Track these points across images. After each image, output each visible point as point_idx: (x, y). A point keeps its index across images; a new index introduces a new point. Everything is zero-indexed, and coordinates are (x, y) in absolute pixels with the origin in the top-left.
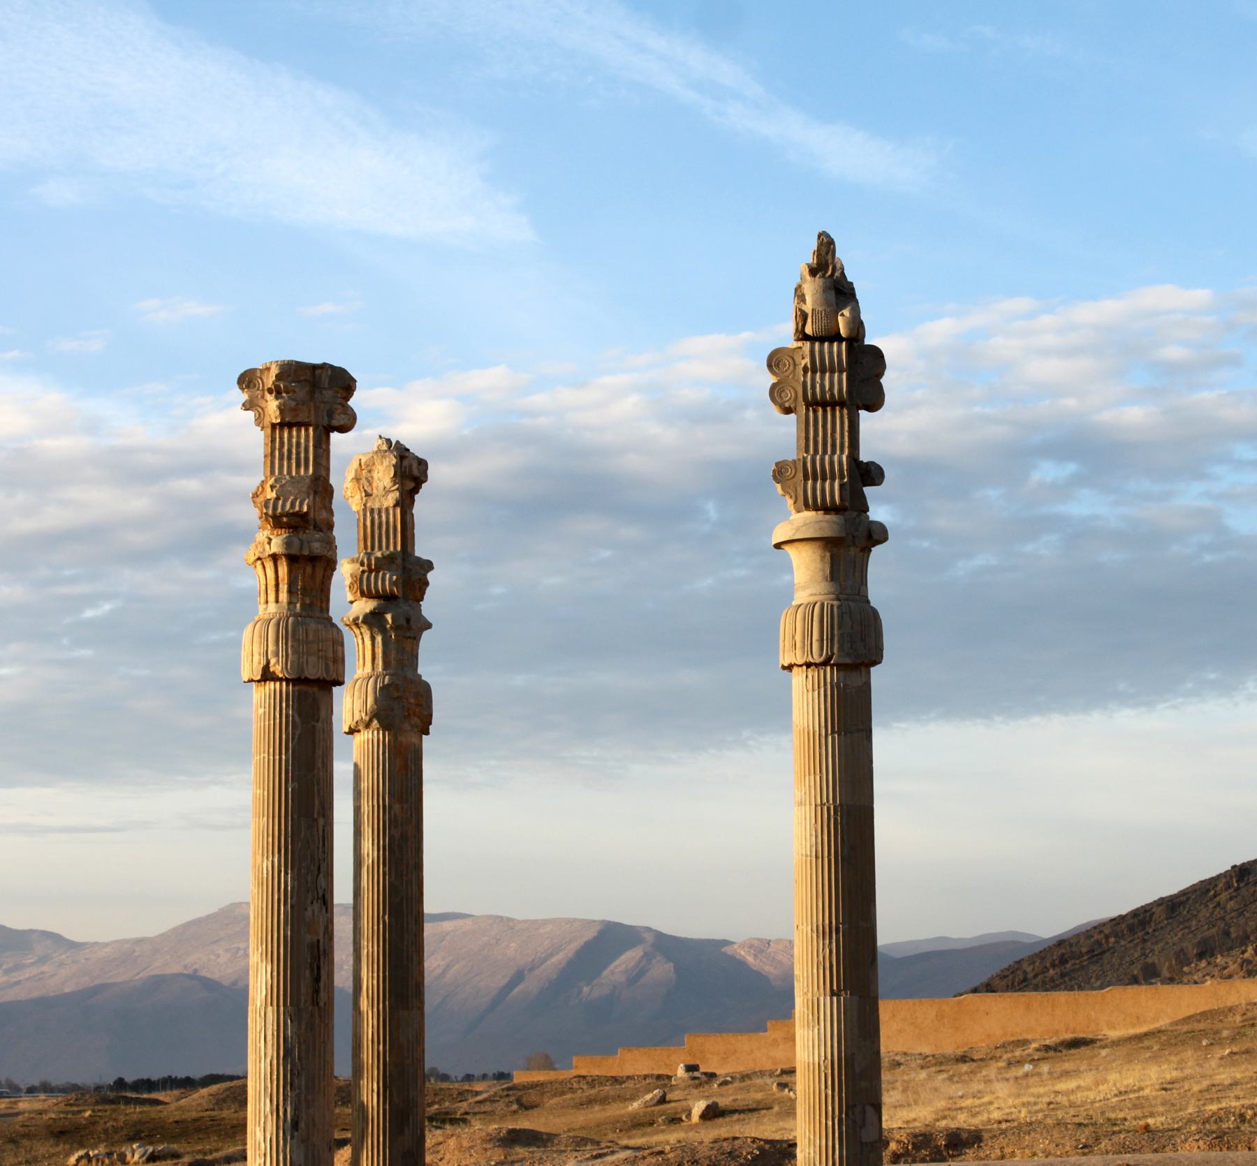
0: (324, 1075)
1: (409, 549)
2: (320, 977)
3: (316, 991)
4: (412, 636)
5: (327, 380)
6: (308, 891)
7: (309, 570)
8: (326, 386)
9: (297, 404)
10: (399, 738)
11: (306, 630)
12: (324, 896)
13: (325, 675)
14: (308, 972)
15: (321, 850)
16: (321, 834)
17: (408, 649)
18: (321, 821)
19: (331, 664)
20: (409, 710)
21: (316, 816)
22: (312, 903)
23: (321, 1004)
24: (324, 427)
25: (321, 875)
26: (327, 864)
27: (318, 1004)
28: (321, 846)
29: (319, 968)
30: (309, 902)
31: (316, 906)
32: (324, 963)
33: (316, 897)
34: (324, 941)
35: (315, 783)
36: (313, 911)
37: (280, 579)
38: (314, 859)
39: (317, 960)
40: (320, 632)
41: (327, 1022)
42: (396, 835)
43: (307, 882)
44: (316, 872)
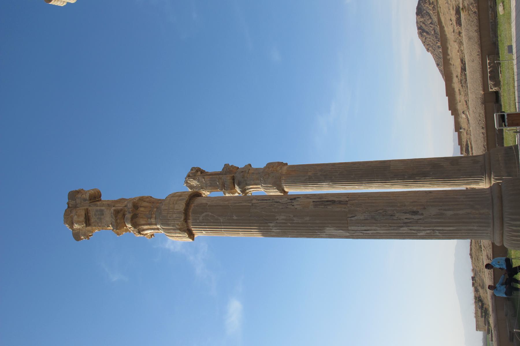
0: (387, 197)
2: (333, 200)
3: (340, 202)
4: (248, 170)
5: (73, 201)
6: (287, 208)
8: (75, 202)
9: (76, 215)
10: (284, 173)
11: (163, 210)
12: (291, 199)
14: (329, 207)
15: (268, 202)
16: (259, 201)
17: (252, 171)
18: (254, 201)
19: (181, 198)
20: (274, 170)
21: (250, 204)
22: (293, 205)
23: (347, 199)
25: (280, 201)
26: (276, 198)
27: (347, 201)
28: (266, 201)
29: (327, 201)
30: (292, 207)
31: (295, 203)
32: (326, 198)
33: (290, 203)
34: (315, 199)
35: (235, 205)
36: (297, 205)
37: (146, 223)
39: (323, 202)
40: (166, 203)
41: (358, 196)
42: (320, 174)
43: (282, 208)
44: (278, 204)
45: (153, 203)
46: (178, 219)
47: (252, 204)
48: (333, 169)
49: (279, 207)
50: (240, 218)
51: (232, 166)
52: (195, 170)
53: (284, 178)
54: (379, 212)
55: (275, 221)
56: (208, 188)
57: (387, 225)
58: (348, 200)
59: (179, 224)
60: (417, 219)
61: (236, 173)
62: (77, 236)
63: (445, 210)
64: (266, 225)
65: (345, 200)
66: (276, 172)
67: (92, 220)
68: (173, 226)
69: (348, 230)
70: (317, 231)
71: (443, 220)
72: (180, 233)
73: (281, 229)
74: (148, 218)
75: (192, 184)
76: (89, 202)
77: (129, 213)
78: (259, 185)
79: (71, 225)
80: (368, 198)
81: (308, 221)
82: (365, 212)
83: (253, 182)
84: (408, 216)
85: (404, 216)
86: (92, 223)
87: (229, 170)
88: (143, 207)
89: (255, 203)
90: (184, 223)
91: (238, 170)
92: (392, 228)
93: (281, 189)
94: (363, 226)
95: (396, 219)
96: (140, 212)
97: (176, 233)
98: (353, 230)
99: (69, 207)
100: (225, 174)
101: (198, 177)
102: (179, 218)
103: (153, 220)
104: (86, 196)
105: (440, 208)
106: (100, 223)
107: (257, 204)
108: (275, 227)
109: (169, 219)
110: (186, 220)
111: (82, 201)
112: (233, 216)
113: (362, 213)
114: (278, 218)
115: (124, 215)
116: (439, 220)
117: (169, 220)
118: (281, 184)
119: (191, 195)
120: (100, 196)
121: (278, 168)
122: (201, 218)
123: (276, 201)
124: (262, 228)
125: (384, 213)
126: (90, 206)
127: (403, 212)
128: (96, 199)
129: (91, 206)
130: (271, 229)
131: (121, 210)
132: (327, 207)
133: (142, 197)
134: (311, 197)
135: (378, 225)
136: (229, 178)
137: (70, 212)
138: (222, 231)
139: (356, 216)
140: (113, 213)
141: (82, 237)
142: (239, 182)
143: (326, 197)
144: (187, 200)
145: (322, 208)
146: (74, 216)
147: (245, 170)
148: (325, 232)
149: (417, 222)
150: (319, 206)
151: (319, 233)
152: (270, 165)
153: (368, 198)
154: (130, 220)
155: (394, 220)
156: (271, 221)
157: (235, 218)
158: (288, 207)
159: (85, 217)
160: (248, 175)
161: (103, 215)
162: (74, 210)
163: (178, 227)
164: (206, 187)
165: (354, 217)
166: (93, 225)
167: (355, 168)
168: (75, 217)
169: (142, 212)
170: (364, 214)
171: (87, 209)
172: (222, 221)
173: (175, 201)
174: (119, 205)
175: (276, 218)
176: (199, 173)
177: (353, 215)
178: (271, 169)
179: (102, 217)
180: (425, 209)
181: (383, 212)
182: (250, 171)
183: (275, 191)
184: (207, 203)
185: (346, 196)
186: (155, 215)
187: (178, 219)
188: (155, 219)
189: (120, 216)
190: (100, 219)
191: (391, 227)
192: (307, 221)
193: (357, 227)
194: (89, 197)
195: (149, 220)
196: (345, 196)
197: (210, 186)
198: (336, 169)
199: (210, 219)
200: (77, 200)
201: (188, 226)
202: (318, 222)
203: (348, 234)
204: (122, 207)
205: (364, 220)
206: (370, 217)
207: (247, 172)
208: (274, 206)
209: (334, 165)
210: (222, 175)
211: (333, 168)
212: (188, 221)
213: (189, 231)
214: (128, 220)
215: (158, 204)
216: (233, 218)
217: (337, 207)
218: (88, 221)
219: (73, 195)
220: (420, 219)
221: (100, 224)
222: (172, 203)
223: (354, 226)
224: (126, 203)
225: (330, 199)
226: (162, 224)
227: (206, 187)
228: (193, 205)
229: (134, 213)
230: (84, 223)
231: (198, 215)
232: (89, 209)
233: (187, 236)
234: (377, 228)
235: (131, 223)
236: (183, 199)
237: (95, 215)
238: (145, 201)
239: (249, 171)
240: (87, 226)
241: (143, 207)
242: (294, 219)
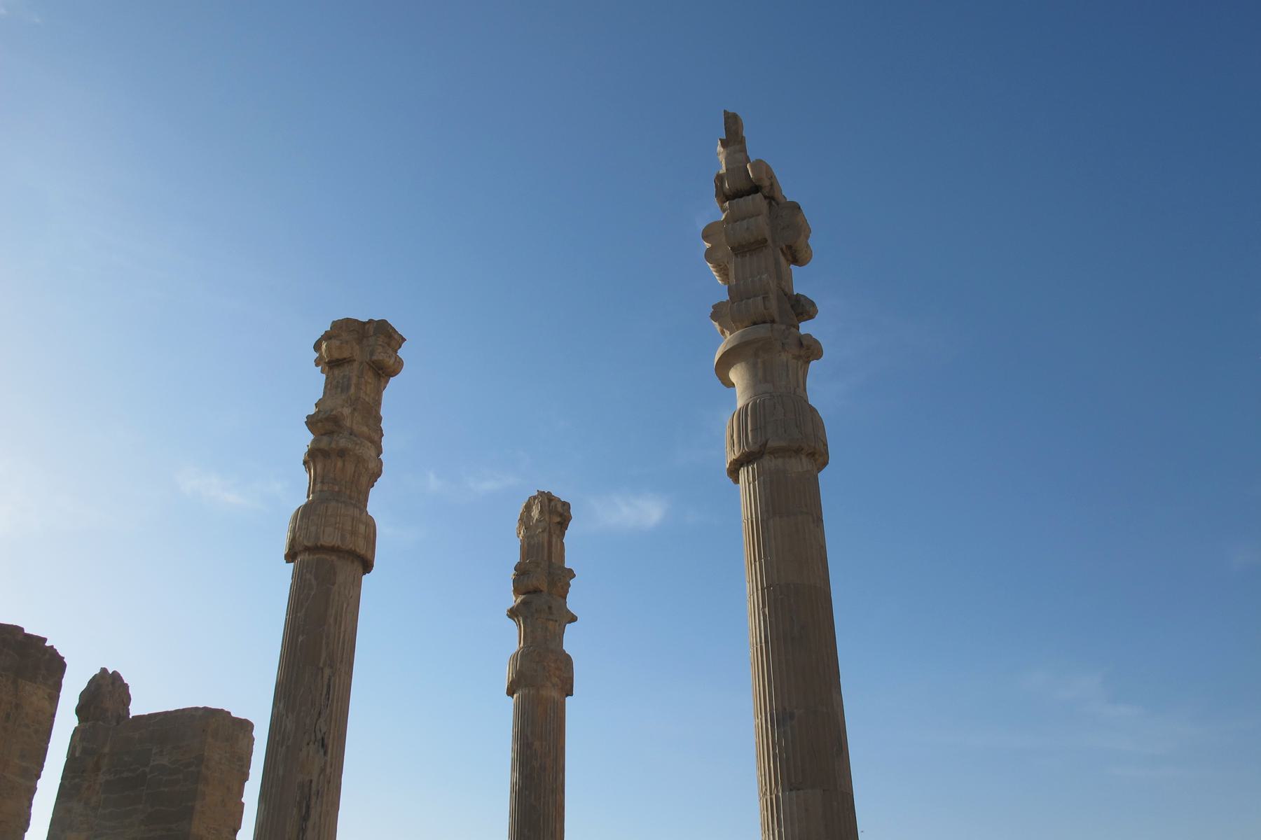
6: (305, 733)
7: (340, 464)
8: (372, 333)
9: (341, 343)
11: (327, 507)
12: (323, 739)
13: (340, 543)
16: (325, 683)
18: (327, 671)
19: (348, 536)
21: (321, 665)
22: (308, 744)
25: (322, 720)
28: (325, 692)
33: (313, 738)
38: (315, 704)
47: (322, 669)
52: (562, 511)
55: (285, 713)
67: (336, 372)
76: (367, 361)
87: (560, 578)
88: (344, 465)
89: (322, 672)
93: (514, 687)
99: (364, 323)
100: (550, 573)
101: (547, 519)
108: (278, 713)
110: (307, 549)
112: (303, 636)
115: (330, 433)
121: (555, 680)
122: (308, 576)
126: (361, 363)
137: (352, 329)
152: (568, 661)
157: (300, 639)
161: (342, 391)
168: (338, 343)
171: (355, 360)
176: (558, 519)
178: (553, 665)
182: (551, 622)
184: (336, 585)
197: (529, 544)
201: (300, 552)
208: (312, 711)
221: (331, 387)
228: (334, 558)
238: (356, 466)
239: (552, 620)
241: (344, 465)
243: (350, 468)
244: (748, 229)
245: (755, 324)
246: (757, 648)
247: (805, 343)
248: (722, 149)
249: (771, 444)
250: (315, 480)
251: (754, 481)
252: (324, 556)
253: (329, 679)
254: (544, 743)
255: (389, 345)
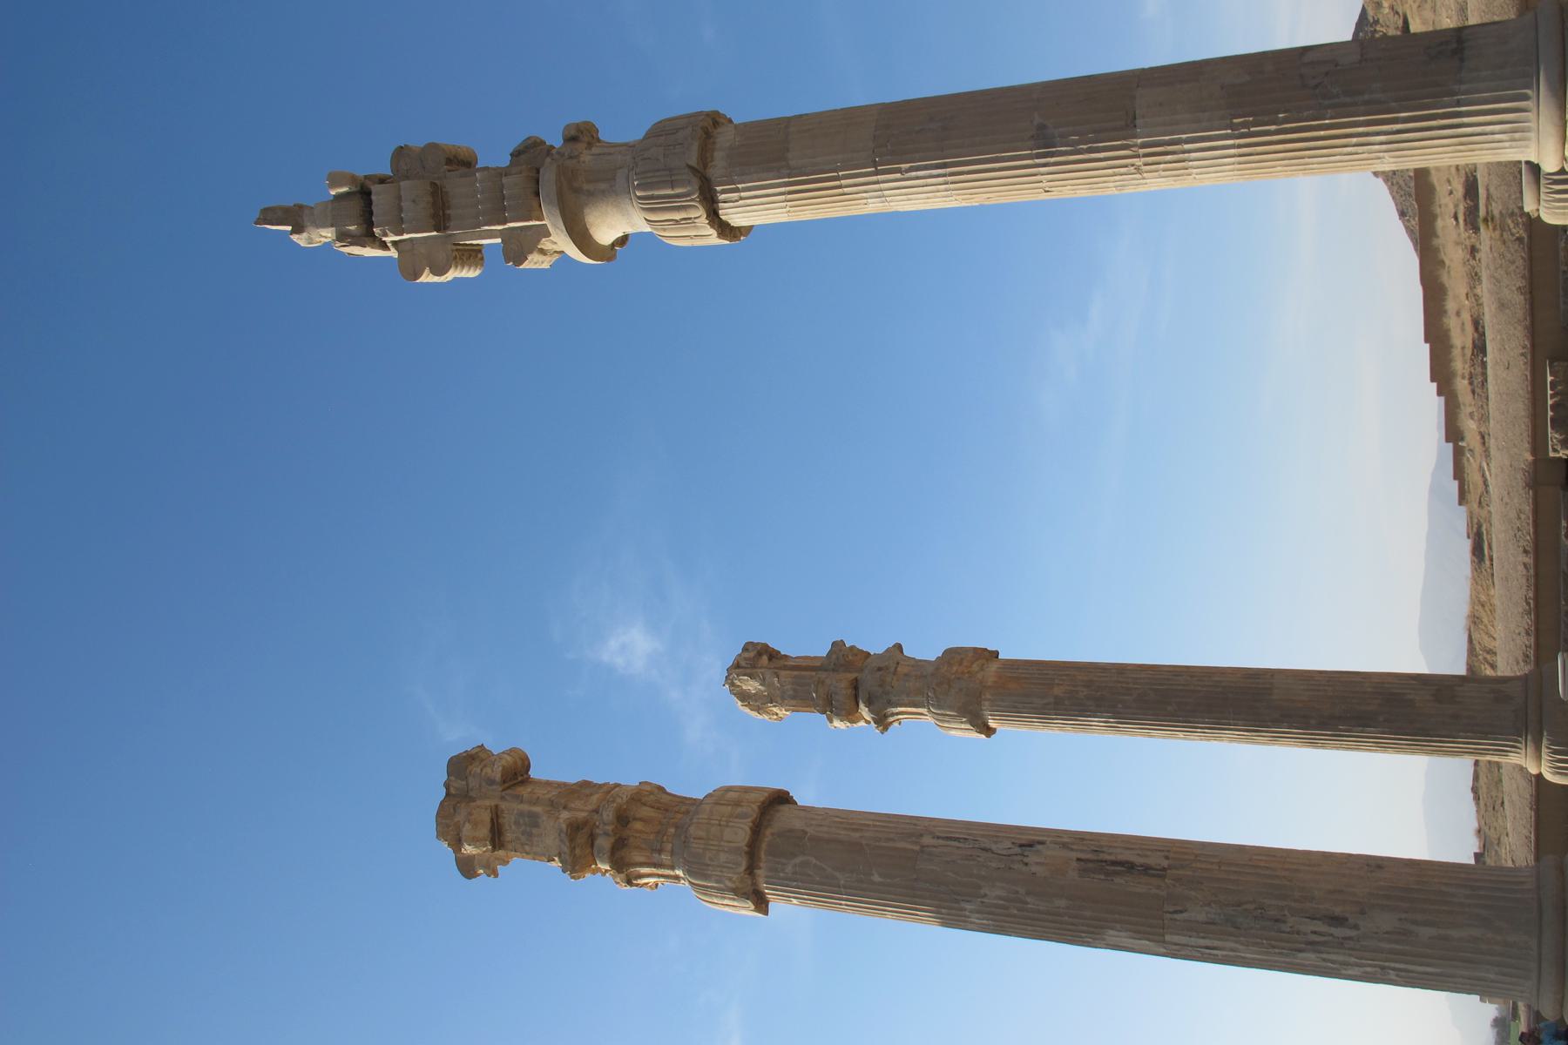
0: (1267, 868)
1: (818, 664)
2: (1127, 862)
3: (1146, 870)
4: (895, 665)
6: (1010, 868)
7: (638, 825)
8: (464, 783)
9: (469, 822)
10: (989, 684)
11: (694, 838)
12: (1021, 846)
13: (749, 820)
14: (1118, 880)
15: (961, 845)
16: (941, 842)
17: (905, 670)
18: (927, 840)
19: (739, 810)
20: (963, 673)
21: (917, 848)
22: (1026, 864)
23: (1165, 863)
24: (503, 790)
25: (994, 847)
27: (1164, 869)
28: (956, 844)
29: (1114, 863)
30: (1024, 868)
32: (1110, 854)
33: (1019, 858)
34: (1081, 851)
35: (877, 844)
37: (647, 861)
38: (971, 856)
39: (1104, 864)
40: (700, 821)
41: (1192, 857)
42: (1085, 693)
43: (999, 868)
44: (989, 855)
45: (667, 810)
46: (730, 865)
47: (923, 847)
48: (1119, 685)
49: (989, 864)
50: (889, 881)
51: (852, 648)
52: (755, 652)
53: (988, 696)
54: (1245, 907)
55: (979, 900)
56: (786, 701)
57: (1265, 941)
58: (1166, 866)
59: (734, 879)
60: (1343, 938)
61: (861, 670)
62: (467, 868)
63: (1415, 922)
64: (956, 905)
65: (1160, 865)
66: (970, 677)
67: (509, 836)
68: (717, 882)
69: (1164, 942)
70: (1083, 935)
71: (1407, 948)
72: (734, 899)
73: (995, 921)
74: (653, 850)
75: (744, 688)
76: (500, 789)
77: (606, 834)
78: (923, 707)
79: (456, 844)
80: (1220, 867)
81: (1063, 908)
82: (1209, 905)
83: (906, 699)
84: (1321, 927)
85: (1309, 926)
86: (509, 842)
87: (844, 658)
88: (641, 819)
89: (928, 846)
90: (746, 876)
91: (869, 660)
92: (1277, 951)
93: (980, 722)
94: (1203, 938)
95: (1289, 930)
96: (635, 834)
97: (725, 898)
98: (1176, 944)
99: (448, 794)
100: (833, 670)
101: (763, 670)
102: (734, 864)
103: (665, 858)
104: (493, 771)
105: (1404, 916)
106: (527, 844)
107: (934, 849)
108: (978, 912)
109: (709, 863)
110: (751, 869)
111: (484, 784)
112: (873, 875)
113: (1201, 906)
114: (988, 893)
115: (592, 838)
116: (1397, 947)
117: (708, 865)
118: (981, 710)
119: (763, 803)
120: (527, 766)
121: (975, 667)
122: (789, 869)
123: (983, 845)
124: (943, 911)
125: (1260, 911)
126: (502, 798)
127: (1307, 915)
128: (517, 779)
129: (506, 800)
130: (969, 917)
131: (585, 823)
132: (1112, 880)
133: (637, 793)
134: (1073, 844)
135: (1242, 939)
136: (843, 685)
137: (452, 810)
138: (841, 904)
139: (1186, 911)
140: (565, 831)
141: (481, 871)
142: (869, 697)
143: (1110, 851)
144: (756, 819)
145: (1100, 879)
146: (464, 823)
147: (887, 663)
148: (1104, 940)
149: (1341, 944)
150: (1092, 875)
151: (1090, 940)
152: (952, 655)
153: (1220, 867)
154: (609, 854)
155: (1284, 932)
156: (969, 899)
157: (876, 878)
158: (1012, 866)
159: (491, 828)
160: (895, 678)
161: (536, 825)
162: (463, 805)
163: (729, 884)
164: (783, 699)
165: (1181, 912)
166: (510, 846)
167: (1179, 685)
168: (468, 826)
169: (638, 835)
170: (1206, 908)
171: (497, 806)
172: (842, 882)
173: (723, 819)
174: (577, 804)
175: (982, 892)
176: (765, 658)
177: (1179, 908)
178: (955, 668)
179: (535, 831)
180: (1363, 912)
181: (1256, 909)
182: (899, 669)
183: (963, 726)
184: (808, 829)
185: (1163, 854)
186: (670, 845)
187: (730, 865)
188: (672, 853)
189: (582, 838)
190: (530, 835)
191: (1274, 947)
192: (1059, 908)
193: (1188, 938)
194: (502, 776)
195: (656, 855)
196: (1160, 851)
197: (793, 698)
198: (1128, 683)
199: (811, 873)
200: (470, 779)
201: (754, 884)
202: (1088, 913)
203: (1165, 951)
204: (587, 811)
205: (1207, 923)
206: (1222, 917)
207: (892, 670)
208: (979, 859)
209: (1121, 669)
210: (826, 670)
211: (1120, 682)
212: (755, 871)
213: (756, 895)
214: (604, 854)
215: (679, 816)
216: (872, 877)
217: (1139, 883)
218: (497, 838)
219: (462, 765)
220: (1350, 938)
221: (530, 847)
222: (717, 822)
223: (1178, 934)
224: (595, 798)
225: (1120, 858)
226: (689, 872)
227: (783, 699)
228: (768, 832)
229: (618, 835)
230: (488, 842)
231: (784, 861)
232: (503, 807)
233: (753, 907)
234: (1237, 946)
235: (609, 862)
236: (745, 816)
237: (517, 823)
238: (645, 804)
239: (896, 668)
240: (494, 848)
241: (641, 819)
242: (1029, 899)
243: (646, 812)
244: (414, 201)
245: (538, 194)
246: (952, 183)
247: (573, 133)
248: (305, 235)
249: (693, 162)
250: (656, 865)
251: (737, 190)
252: (764, 846)
253: (938, 838)
254: (1057, 681)
255: (482, 760)
